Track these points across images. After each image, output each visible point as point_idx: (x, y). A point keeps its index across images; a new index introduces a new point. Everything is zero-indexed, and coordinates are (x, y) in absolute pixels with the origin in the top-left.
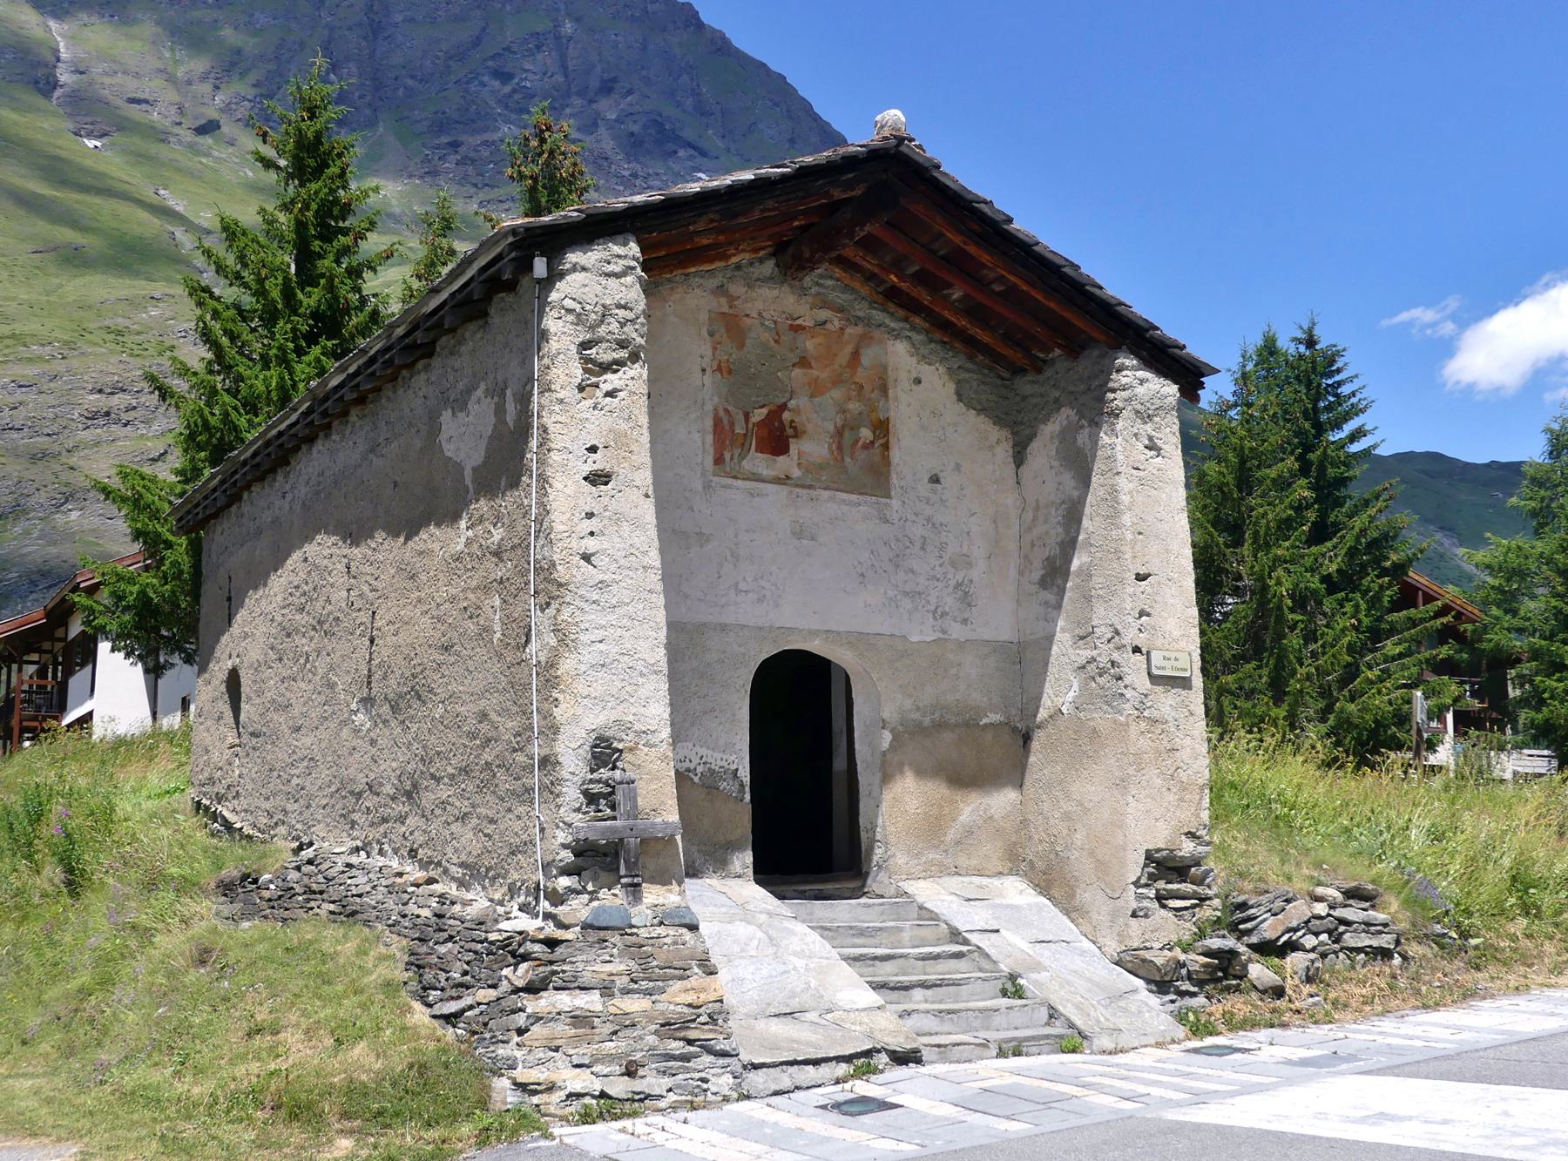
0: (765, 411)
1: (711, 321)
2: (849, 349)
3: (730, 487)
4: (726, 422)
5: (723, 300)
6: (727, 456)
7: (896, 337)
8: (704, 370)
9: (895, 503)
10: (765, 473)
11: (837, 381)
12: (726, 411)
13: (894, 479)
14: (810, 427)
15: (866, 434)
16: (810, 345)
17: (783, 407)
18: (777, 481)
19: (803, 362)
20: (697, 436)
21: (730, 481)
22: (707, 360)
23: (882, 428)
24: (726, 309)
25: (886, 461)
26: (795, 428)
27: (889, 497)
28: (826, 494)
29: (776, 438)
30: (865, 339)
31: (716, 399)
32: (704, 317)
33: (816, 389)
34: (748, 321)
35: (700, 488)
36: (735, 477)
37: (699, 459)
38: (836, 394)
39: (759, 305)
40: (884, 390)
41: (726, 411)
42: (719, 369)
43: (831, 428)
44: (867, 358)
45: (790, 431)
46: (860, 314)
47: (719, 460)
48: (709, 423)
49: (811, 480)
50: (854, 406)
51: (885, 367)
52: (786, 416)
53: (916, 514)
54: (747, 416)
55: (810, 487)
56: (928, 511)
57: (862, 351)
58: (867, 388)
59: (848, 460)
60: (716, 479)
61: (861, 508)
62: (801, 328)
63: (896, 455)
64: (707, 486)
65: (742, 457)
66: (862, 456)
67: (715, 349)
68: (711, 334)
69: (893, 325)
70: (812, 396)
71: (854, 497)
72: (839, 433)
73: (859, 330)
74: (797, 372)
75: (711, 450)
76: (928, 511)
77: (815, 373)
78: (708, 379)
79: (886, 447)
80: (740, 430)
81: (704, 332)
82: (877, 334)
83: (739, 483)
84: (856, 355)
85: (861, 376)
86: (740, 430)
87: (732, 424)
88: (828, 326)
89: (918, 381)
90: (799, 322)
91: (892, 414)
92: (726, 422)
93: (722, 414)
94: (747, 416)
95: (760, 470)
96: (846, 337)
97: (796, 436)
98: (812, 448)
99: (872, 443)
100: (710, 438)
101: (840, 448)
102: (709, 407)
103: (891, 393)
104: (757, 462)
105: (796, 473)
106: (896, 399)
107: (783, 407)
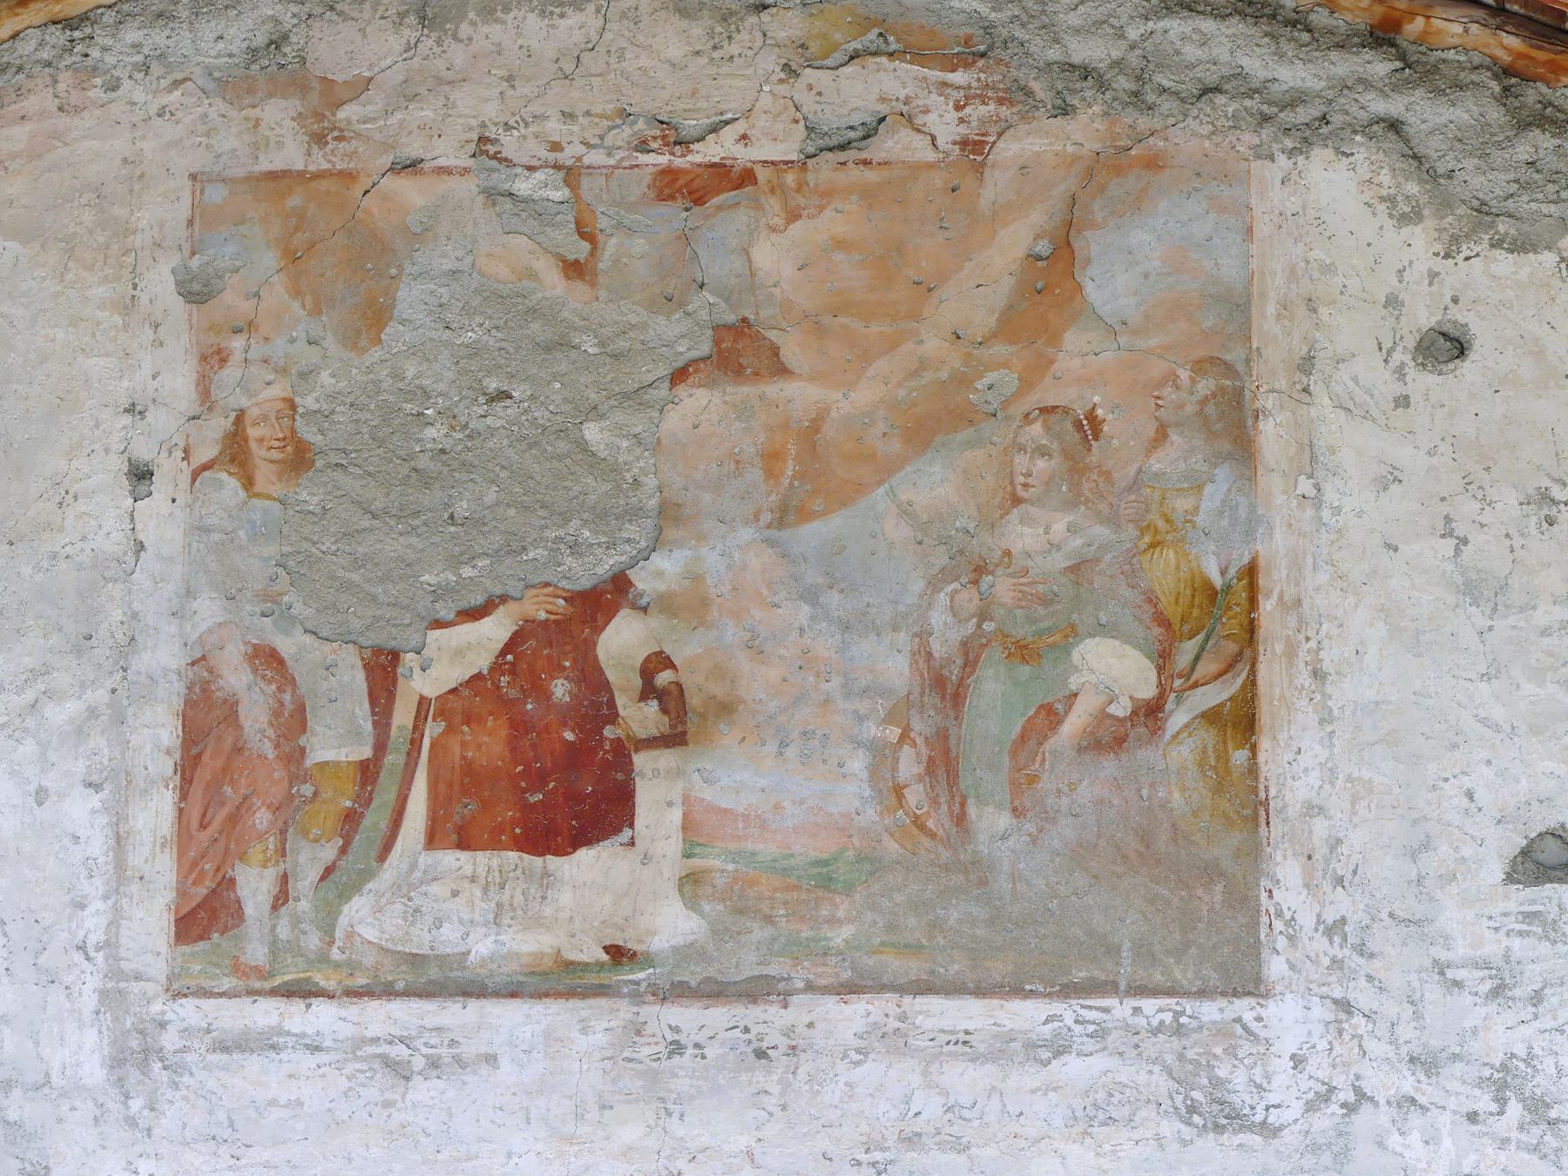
0: (495, 630)
1: (202, 220)
2: (1018, 238)
3: (268, 1043)
4: (255, 717)
5: (278, 114)
6: (254, 886)
7: (1307, 137)
8: (141, 475)
9: (1289, 1018)
10: (482, 947)
11: (933, 421)
12: (267, 659)
13: (1288, 888)
14: (758, 683)
15: (1112, 668)
16: (771, 256)
17: (610, 596)
18: (558, 980)
19: (738, 351)
20: (81, 810)
21: (265, 1013)
22: (163, 422)
23: (1219, 629)
24: (292, 154)
25: (1245, 804)
26: (672, 700)
27: (1253, 986)
28: (850, 1017)
29: (552, 772)
30: (1123, 170)
31: (208, 610)
32: (162, 212)
33: (807, 477)
34: (411, 192)
35: (94, 1072)
36: (302, 991)
37: (93, 923)
38: (934, 483)
39: (479, 104)
40: (1231, 426)
41: (267, 659)
42: (235, 452)
43: (894, 666)
44: (1116, 277)
45: (640, 717)
46: (1093, 51)
47: (203, 917)
48: (156, 733)
49: (772, 946)
50: (1043, 537)
51: (1237, 307)
52: (622, 642)
53: (1426, 1063)
54: (383, 671)
55: (756, 991)
56: (1504, 1034)
57: (1091, 243)
58: (1124, 429)
59: (992, 821)
60: (189, 1011)
61: (1073, 1068)
62: (734, 177)
63: (1295, 761)
64: (135, 1054)
65: (338, 882)
66: (1083, 790)
67: (213, 358)
68: (196, 291)
69: (1294, 74)
70: (788, 514)
71: (1028, 1015)
72: (947, 687)
73: (1086, 130)
74: (699, 403)
75: (164, 870)
76: (1504, 1034)
77: (799, 395)
78: (162, 519)
79: (1241, 722)
80: (336, 743)
81: (160, 283)
82: (1188, 137)
83: (323, 1017)
84: (1054, 272)
85: (1081, 366)
86: (336, 743)
87: (293, 722)
88: (896, 144)
89: (1447, 346)
90: (709, 151)
91: (1275, 547)
92: (255, 717)
93: (236, 677)
94: (383, 671)
95: (449, 938)
96: (996, 186)
97: (674, 739)
98: (767, 786)
99: (1151, 712)
100: (156, 813)
101: (943, 763)
102: (164, 656)
103: (1272, 435)
104: (452, 899)
105: (671, 925)
106: (1309, 458)
107: (610, 596)
